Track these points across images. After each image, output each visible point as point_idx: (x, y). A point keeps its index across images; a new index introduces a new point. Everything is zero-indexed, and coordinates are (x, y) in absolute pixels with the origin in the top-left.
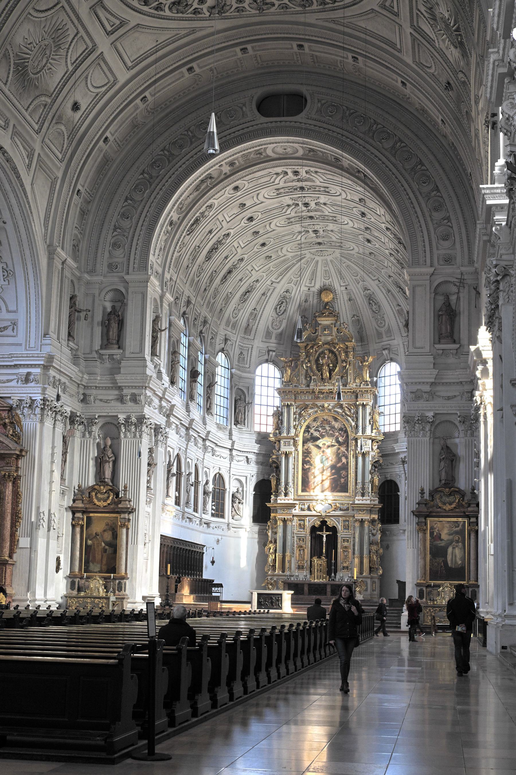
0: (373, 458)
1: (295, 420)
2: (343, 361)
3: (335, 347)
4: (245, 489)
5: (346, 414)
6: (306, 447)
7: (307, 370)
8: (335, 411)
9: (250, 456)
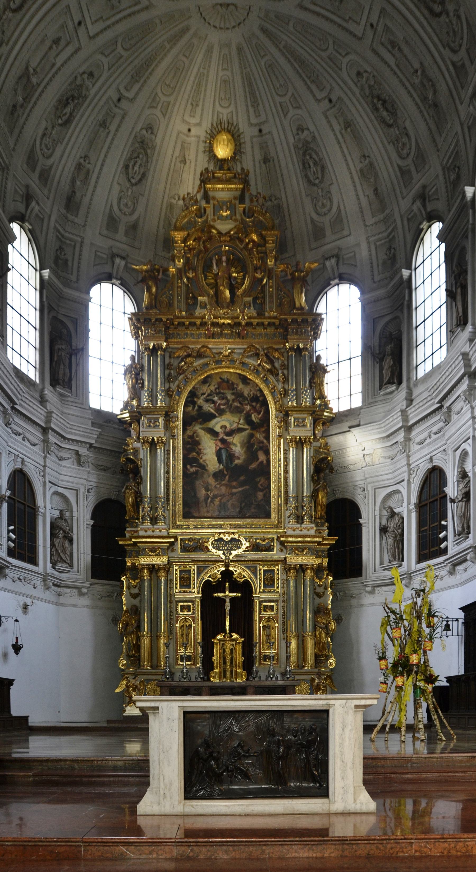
0: (317, 451)
1: (168, 379)
2: (256, 269)
3: (241, 241)
4: (75, 514)
5: (263, 367)
6: (189, 433)
7: (187, 286)
8: (243, 364)
9: (83, 451)
